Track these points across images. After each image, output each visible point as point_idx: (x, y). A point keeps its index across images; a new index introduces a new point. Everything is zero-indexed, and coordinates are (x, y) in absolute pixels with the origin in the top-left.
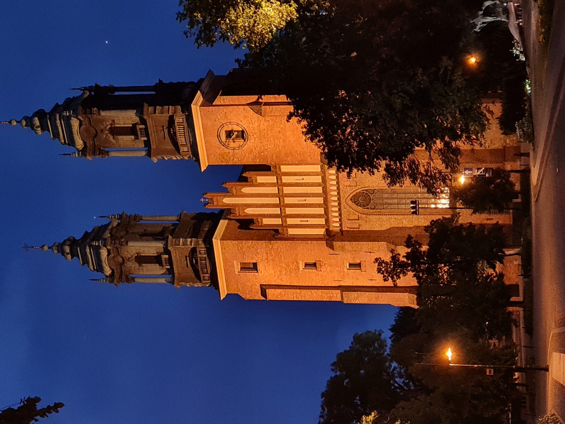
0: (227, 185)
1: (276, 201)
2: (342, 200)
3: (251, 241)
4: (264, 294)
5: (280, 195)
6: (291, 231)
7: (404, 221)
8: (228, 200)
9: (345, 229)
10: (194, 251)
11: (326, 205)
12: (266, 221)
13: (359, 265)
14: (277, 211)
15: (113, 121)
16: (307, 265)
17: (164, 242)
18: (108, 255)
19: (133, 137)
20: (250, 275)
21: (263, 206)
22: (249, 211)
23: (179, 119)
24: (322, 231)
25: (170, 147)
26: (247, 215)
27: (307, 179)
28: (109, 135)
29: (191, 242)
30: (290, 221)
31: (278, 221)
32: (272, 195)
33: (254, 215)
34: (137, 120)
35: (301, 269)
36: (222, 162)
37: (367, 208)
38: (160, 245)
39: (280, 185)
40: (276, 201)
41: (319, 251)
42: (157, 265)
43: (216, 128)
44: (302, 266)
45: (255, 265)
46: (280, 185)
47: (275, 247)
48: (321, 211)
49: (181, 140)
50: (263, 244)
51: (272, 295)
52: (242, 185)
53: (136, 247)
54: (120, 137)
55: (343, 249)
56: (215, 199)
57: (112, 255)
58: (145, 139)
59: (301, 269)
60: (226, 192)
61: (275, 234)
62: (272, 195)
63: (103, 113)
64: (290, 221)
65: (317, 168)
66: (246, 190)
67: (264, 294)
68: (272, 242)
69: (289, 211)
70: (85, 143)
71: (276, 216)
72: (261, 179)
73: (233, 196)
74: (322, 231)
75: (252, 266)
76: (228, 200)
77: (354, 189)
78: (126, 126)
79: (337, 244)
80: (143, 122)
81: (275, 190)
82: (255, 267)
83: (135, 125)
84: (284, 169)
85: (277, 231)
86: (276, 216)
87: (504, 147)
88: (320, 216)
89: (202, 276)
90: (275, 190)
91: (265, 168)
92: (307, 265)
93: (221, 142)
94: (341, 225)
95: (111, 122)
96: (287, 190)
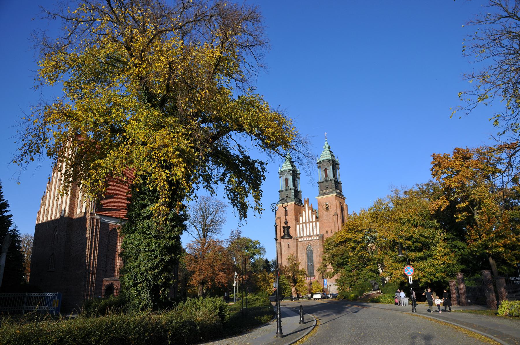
1: (307, 221)
5: (309, 222)
6: (298, 226)
11: (307, 236)
12: (301, 218)
13: (289, 247)
14: (304, 221)
22: (304, 213)
24: (298, 236)
30: (301, 225)
31: (301, 222)
39: (312, 222)
46: (312, 222)
48: (305, 235)
53: (290, 178)
55: (294, 242)
64: (301, 225)
65: (318, 233)
66: (310, 211)
71: (302, 221)
72: (314, 216)
74: (298, 236)
81: (311, 220)
84: (318, 223)
86: (302, 221)
88: (303, 234)
90: (311, 220)
96: (311, 224)
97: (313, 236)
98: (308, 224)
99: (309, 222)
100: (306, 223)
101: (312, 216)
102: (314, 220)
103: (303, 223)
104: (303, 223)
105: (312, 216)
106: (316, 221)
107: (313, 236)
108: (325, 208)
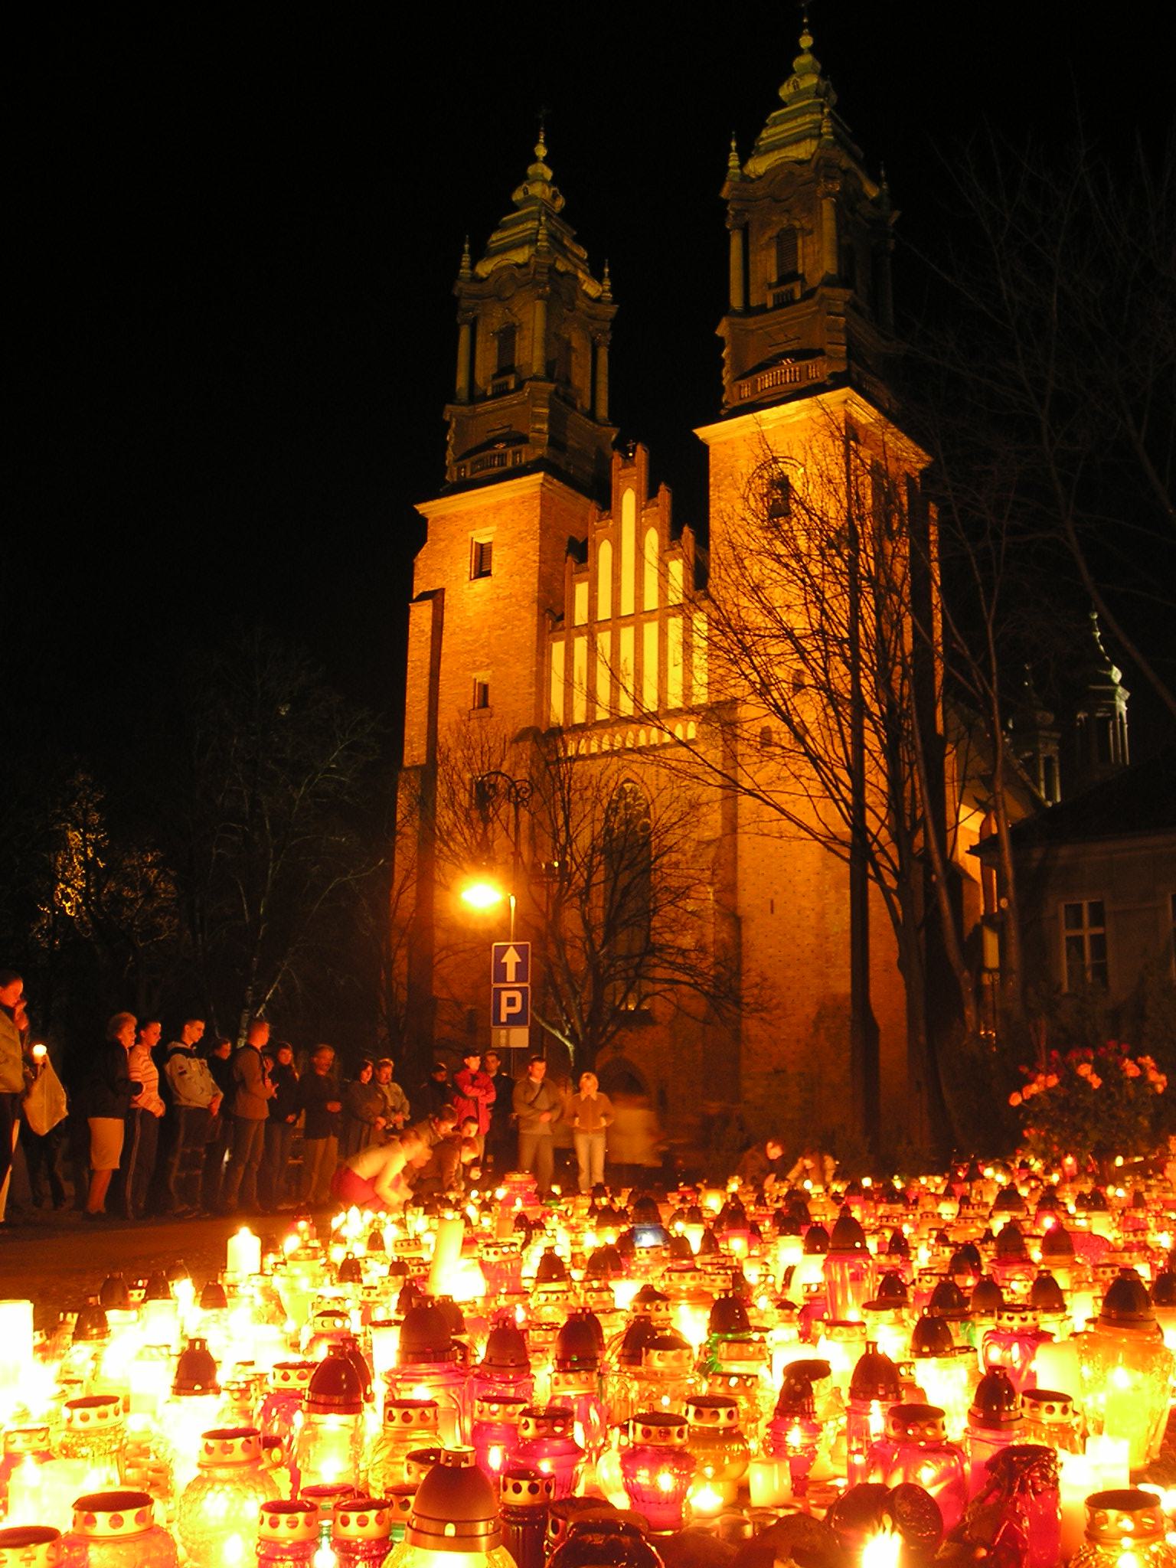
0: (664, 494)
1: (627, 608)
3: (537, 558)
4: (424, 596)
5: (640, 617)
6: (558, 649)
8: (628, 501)
10: (523, 439)
12: (582, 590)
15: (811, 232)
16: (484, 688)
17: (542, 373)
18: (518, 265)
19: (774, 279)
20: (466, 565)
21: (616, 578)
22: (605, 551)
23: (817, 370)
26: (596, 546)
27: (675, 674)
28: (778, 229)
29: (540, 431)
30: (581, 644)
31: (581, 616)
33: (596, 562)
34: (815, 279)
35: (474, 675)
36: (717, 474)
38: (537, 367)
40: (627, 608)
42: (495, 371)
44: (482, 676)
45: (488, 574)
46: (665, 612)
47: (524, 614)
49: (767, 380)
50: (529, 583)
51: (420, 616)
52: (662, 527)
54: (773, 252)
56: (632, 470)
58: (770, 304)
59: (474, 675)
60: (650, 493)
61: (553, 614)
63: (827, 209)
64: (581, 644)
66: (652, 538)
67: (424, 596)
68: (535, 606)
70: (760, 177)
71: (593, 610)
72: (676, 567)
73: (639, 509)
76: (628, 501)
78: (800, 261)
80: (808, 295)
83: (801, 278)
84: (700, 622)
86: (593, 610)
89: (468, 463)
92: (484, 688)
95: (808, 226)
101: (664, 574)
103: (591, 629)
105: (664, 574)
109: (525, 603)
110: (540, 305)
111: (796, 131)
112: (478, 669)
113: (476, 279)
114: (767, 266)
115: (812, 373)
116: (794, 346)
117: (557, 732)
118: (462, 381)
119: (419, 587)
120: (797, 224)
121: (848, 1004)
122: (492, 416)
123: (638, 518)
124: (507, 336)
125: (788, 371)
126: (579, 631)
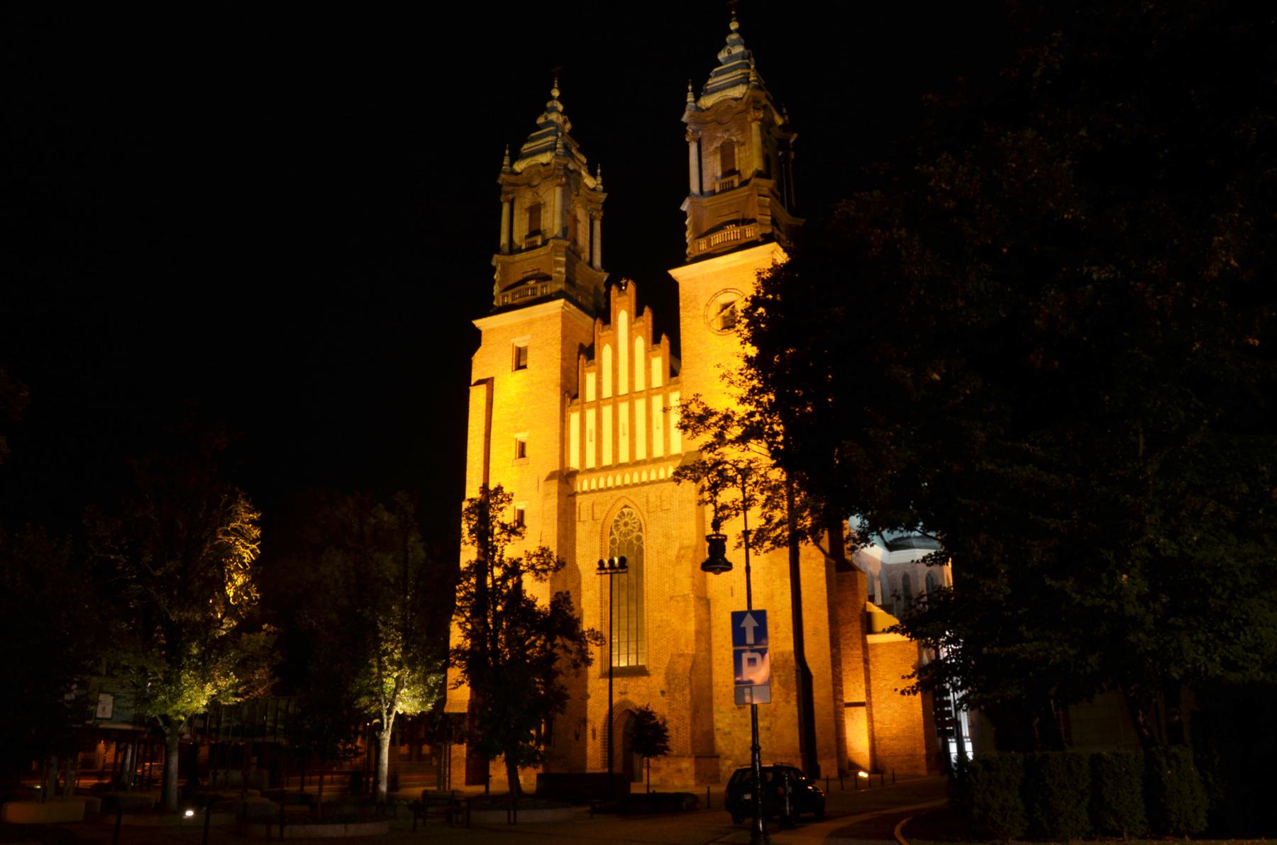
0: (648, 313)
2: (624, 492)
4: (480, 382)
6: (574, 418)
7: (590, 593)
8: (622, 318)
9: (579, 499)
10: (547, 278)
11: (617, 466)
12: (590, 379)
14: (607, 392)
15: (743, 144)
17: (560, 235)
18: (543, 165)
19: (719, 174)
20: (509, 361)
22: (606, 353)
23: (751, 232)
24: (574, 463)
25: (706, 228)
26: (600, 348)
29: (559, 272)
30: (591, 414)
31: (590, 395)
32: (632, 383)
33: (600, 359)
34: (748, 174)
37: (611, 533)
38: (557, 230)
39: (649, 393)
41: (544, 459)
43: (738, 286)
44: (522, 436)
45: (525, 367)
46: (649, 393)
48: (607, 460)
49: (717, 238)
50: (555, 373)
51: (477, 396)
55: (547, 495)
56: (625, 298)
57: (542, 169)
58: (718, 190)
61: (571, 392)
62: (632, 383)
63: (755, 127)
64: (591, 414)
66: (640, 343)
67: (480, 382)
68: (559, 389)
69: (607, 411)
70: (708, 109)
72: (658, 364)
73: (630, 323)
75: (522, 364)
77: (644, 509)
79: (554, 487)
80: (744, 183)
81: (640, 385)
82: (520, 366)
83: (738, 173)
85: (576, 396)
87: (718, 757)
89: (509, 293)
90: (640, 385)
91: (674, 371)
93: (716, 295)
94: (584, 493)
95: (742, 140)
97: (652, 461)
98: (624, 408)
99: (632, 396)
100: (616, 399)
101: (648, 366)
102: (658, 381)
103: (599, 403)
104: (599, 403)
105: (648, 366)
106: (664, 391)
107: (652, 461)
108: (718, 325)
109: (552, 387)
110: (558, 190)
111: (729, 85)
112: (518, 431)
113: (514, 173)
114: (714, 167)
115: (748, 234)
116: (734, 217)
117: (573, 474)
118: (504, 240)
119: (476, 376)
120: (734, 139)
121: (793, 658)
122: (524, 264)
123: (630, 330)
124: (535, 211)
125: (732, 233)
126: (591, 405)
